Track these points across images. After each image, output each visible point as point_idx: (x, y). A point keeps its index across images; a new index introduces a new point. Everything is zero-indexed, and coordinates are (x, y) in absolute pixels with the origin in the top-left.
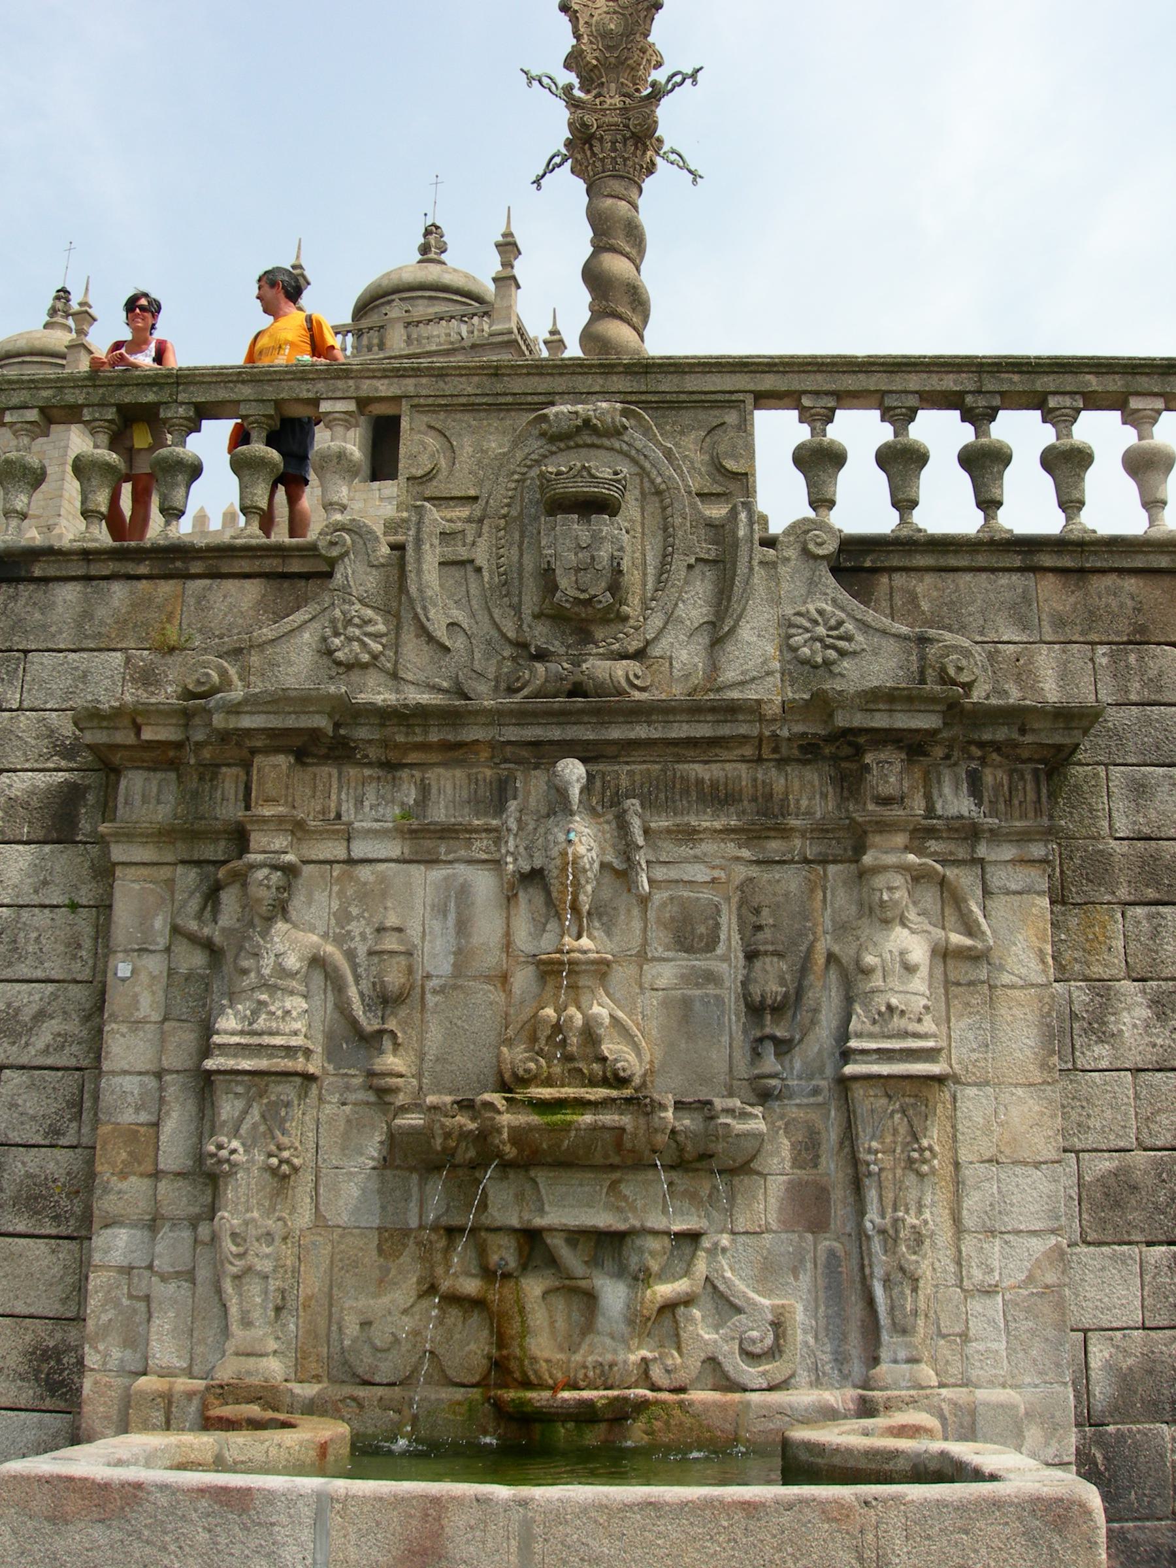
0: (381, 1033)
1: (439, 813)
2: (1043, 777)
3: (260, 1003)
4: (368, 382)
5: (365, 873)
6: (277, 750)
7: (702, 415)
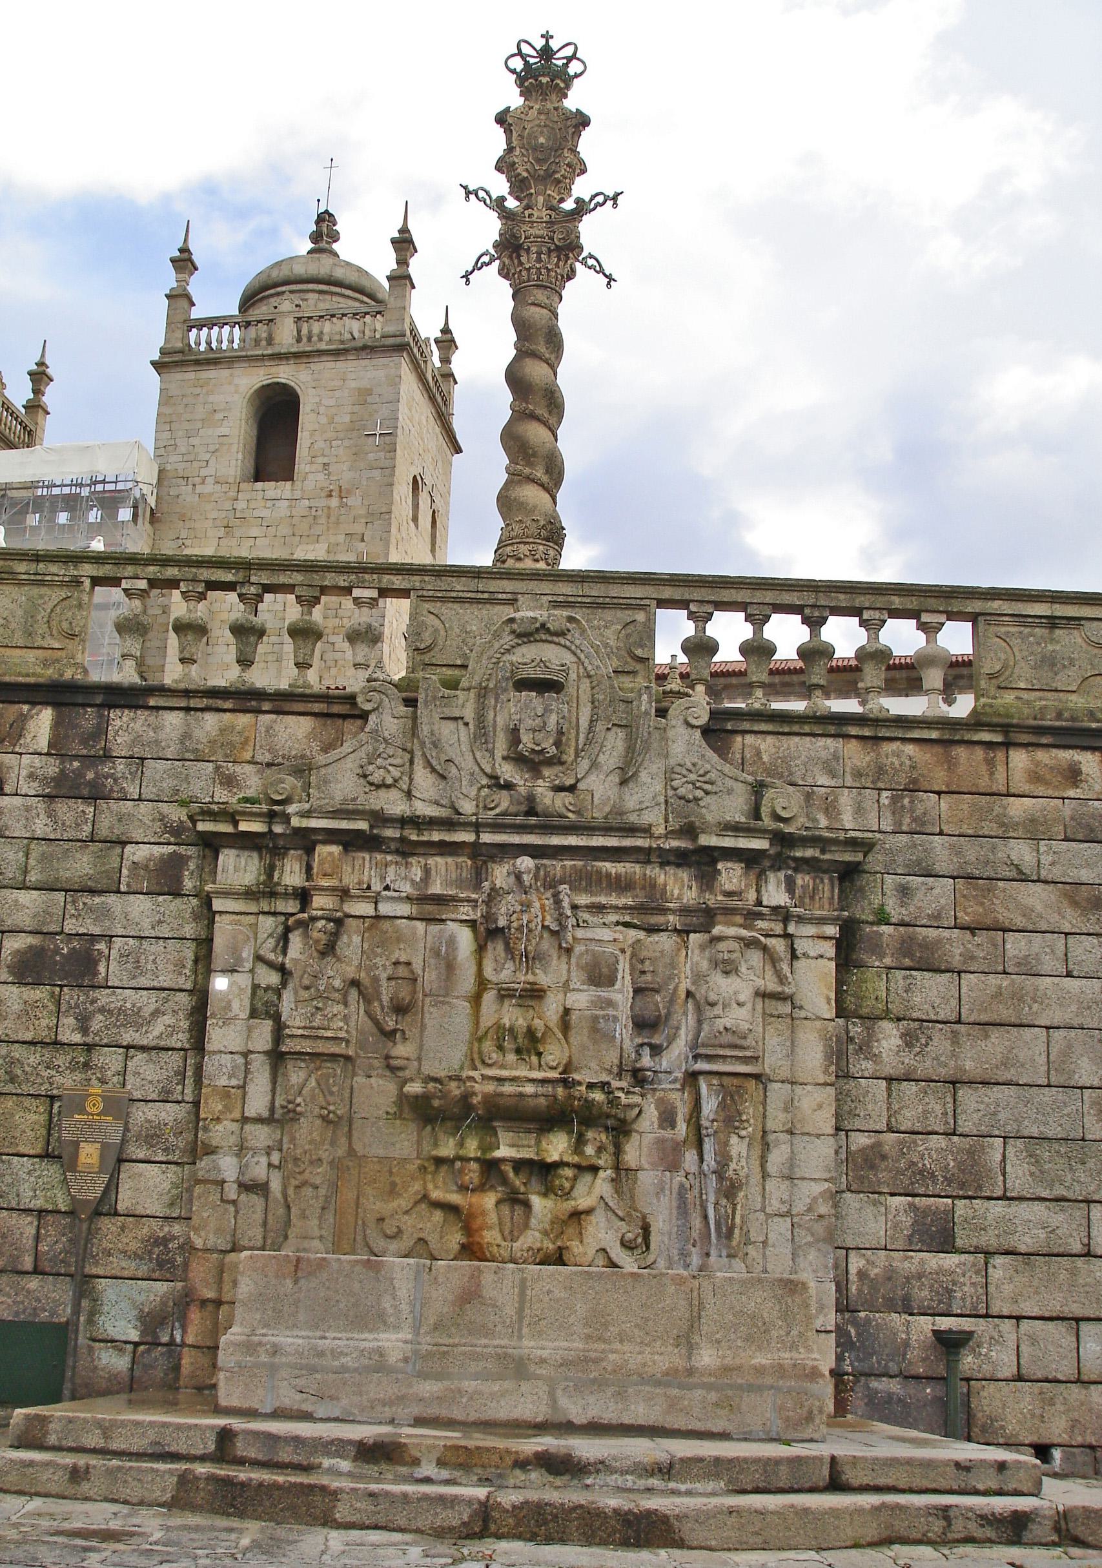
0: (395, 1031)
1: (436, 889)
2: (836, 883)
3: (317, 1008)
4: (387, 577)
5: (385, 925)
6: (332, 842)
7: (619, 614)
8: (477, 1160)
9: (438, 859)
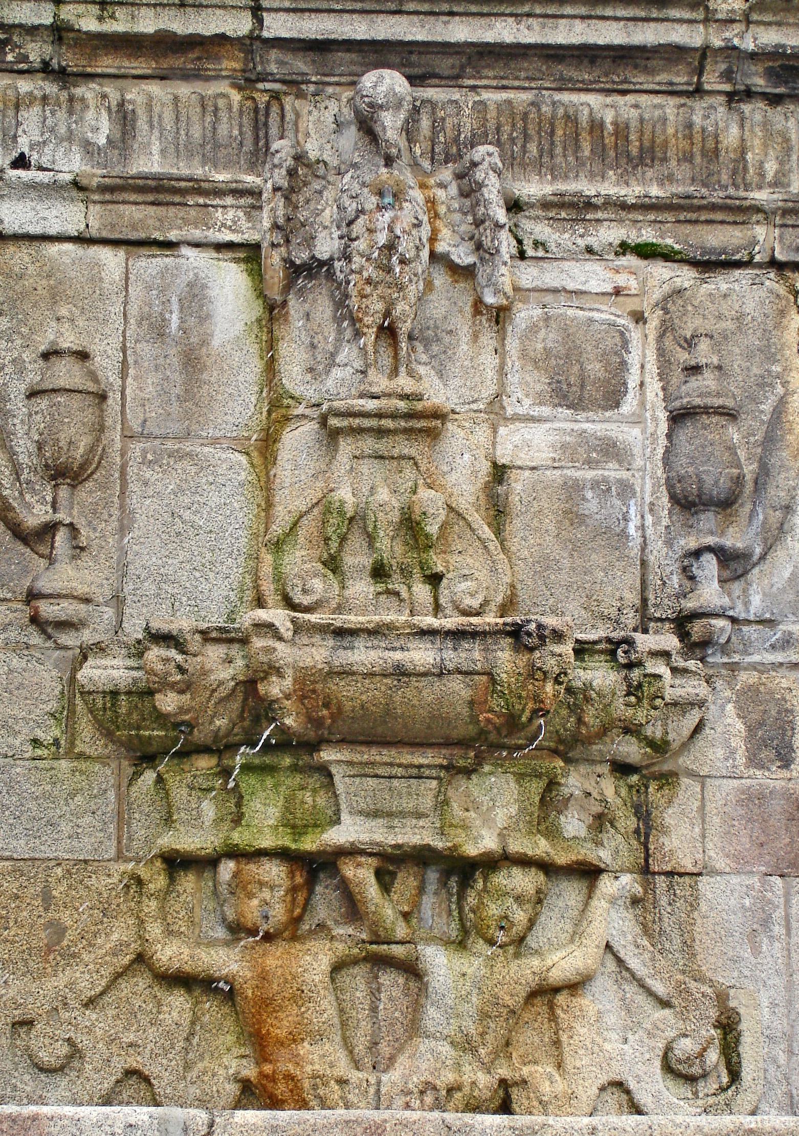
0: (50, 528)
1: (150, 161)
8: (282, 854)
9: (155, 88)
